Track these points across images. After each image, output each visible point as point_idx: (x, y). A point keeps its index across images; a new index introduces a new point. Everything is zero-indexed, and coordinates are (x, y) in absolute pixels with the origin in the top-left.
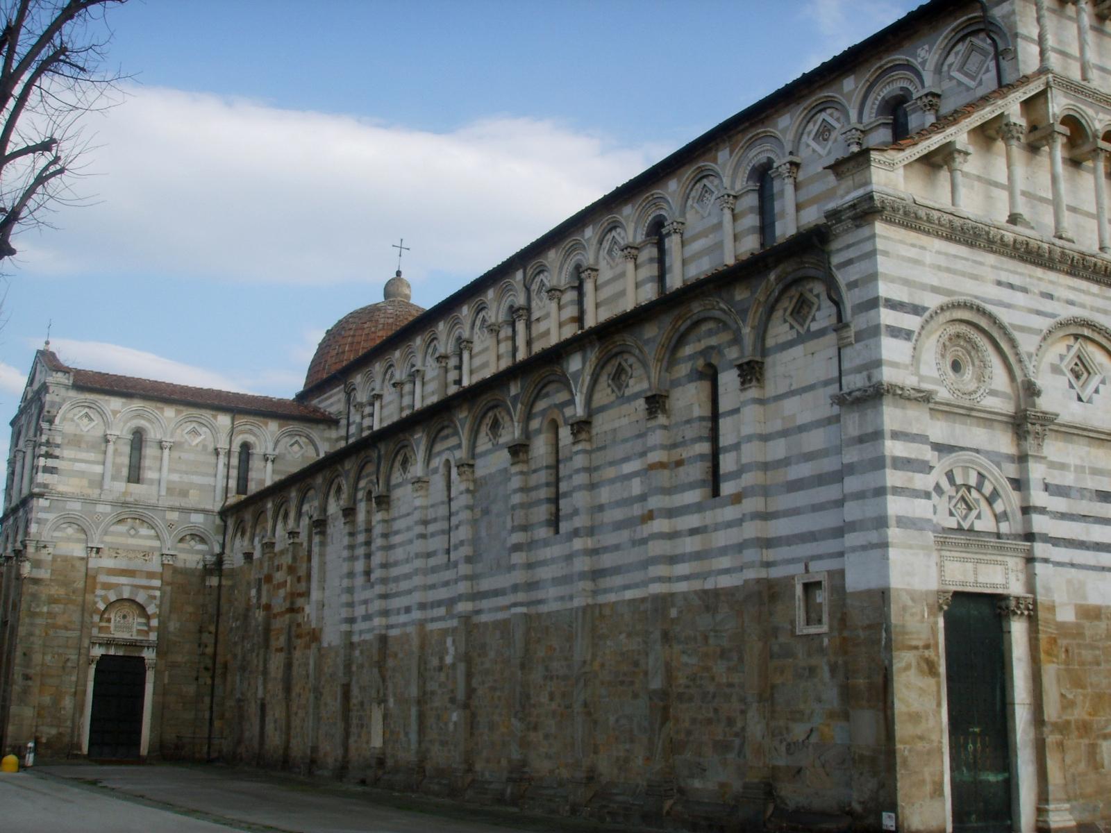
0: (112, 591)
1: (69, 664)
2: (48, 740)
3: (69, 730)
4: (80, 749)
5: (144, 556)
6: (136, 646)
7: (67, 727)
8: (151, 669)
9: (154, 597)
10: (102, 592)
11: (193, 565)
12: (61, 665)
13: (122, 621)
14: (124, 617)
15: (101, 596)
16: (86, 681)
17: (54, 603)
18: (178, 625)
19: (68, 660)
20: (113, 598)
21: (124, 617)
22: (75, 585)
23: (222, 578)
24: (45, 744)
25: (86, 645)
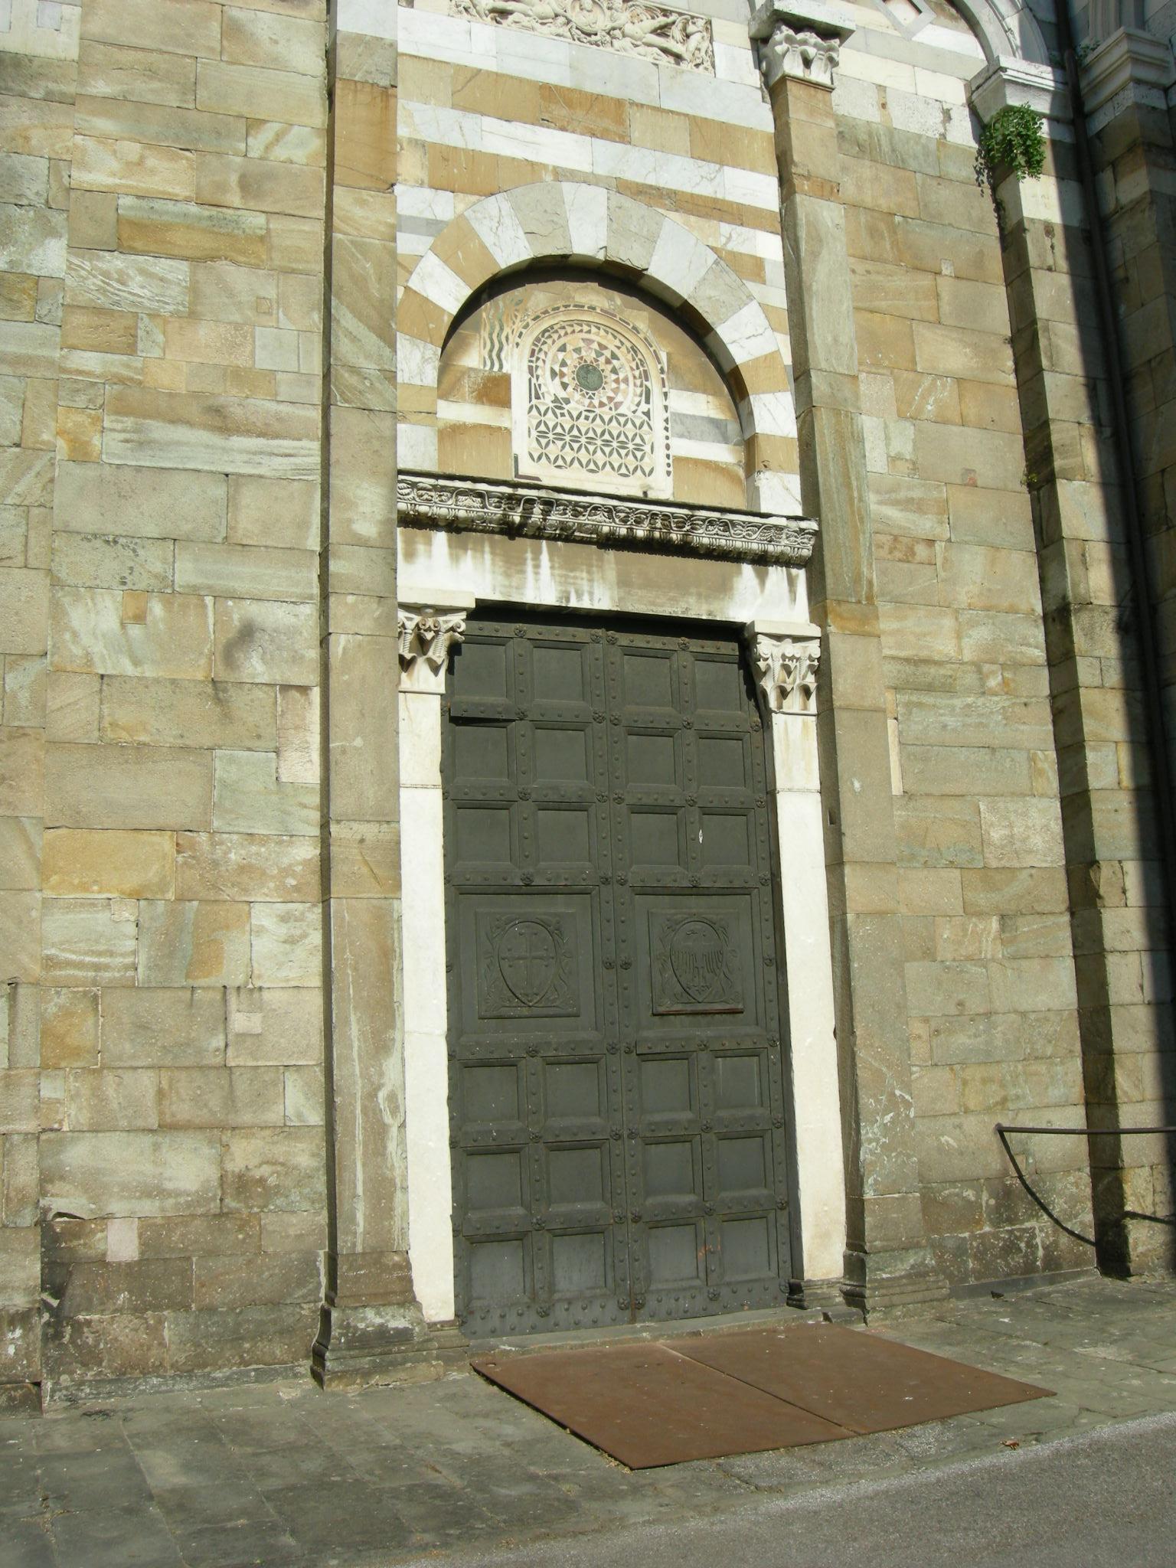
0: (493, 205)
1: (255, 667)
2: (152, 1236)
3: (306, 1156)
4: (406, 1298)
5: (662, 31)
6: (686, 550)
7: (285, 1131)
8: (794, 702)
9: (755, 268)
10: (444, 206)
11: (928, 124)
12: (196, 671)
13: (578, 403)
14: (589, 377)
15: (433, 227)
16: (393, 787)
17: (120, 247)
18: (903, 441)
19: (247, 633)
20: (513, 251)
21: (589, 377)
22: (257, 144)
23: (1107, 176)
24: (132, 1272)
25: (367, 528)
